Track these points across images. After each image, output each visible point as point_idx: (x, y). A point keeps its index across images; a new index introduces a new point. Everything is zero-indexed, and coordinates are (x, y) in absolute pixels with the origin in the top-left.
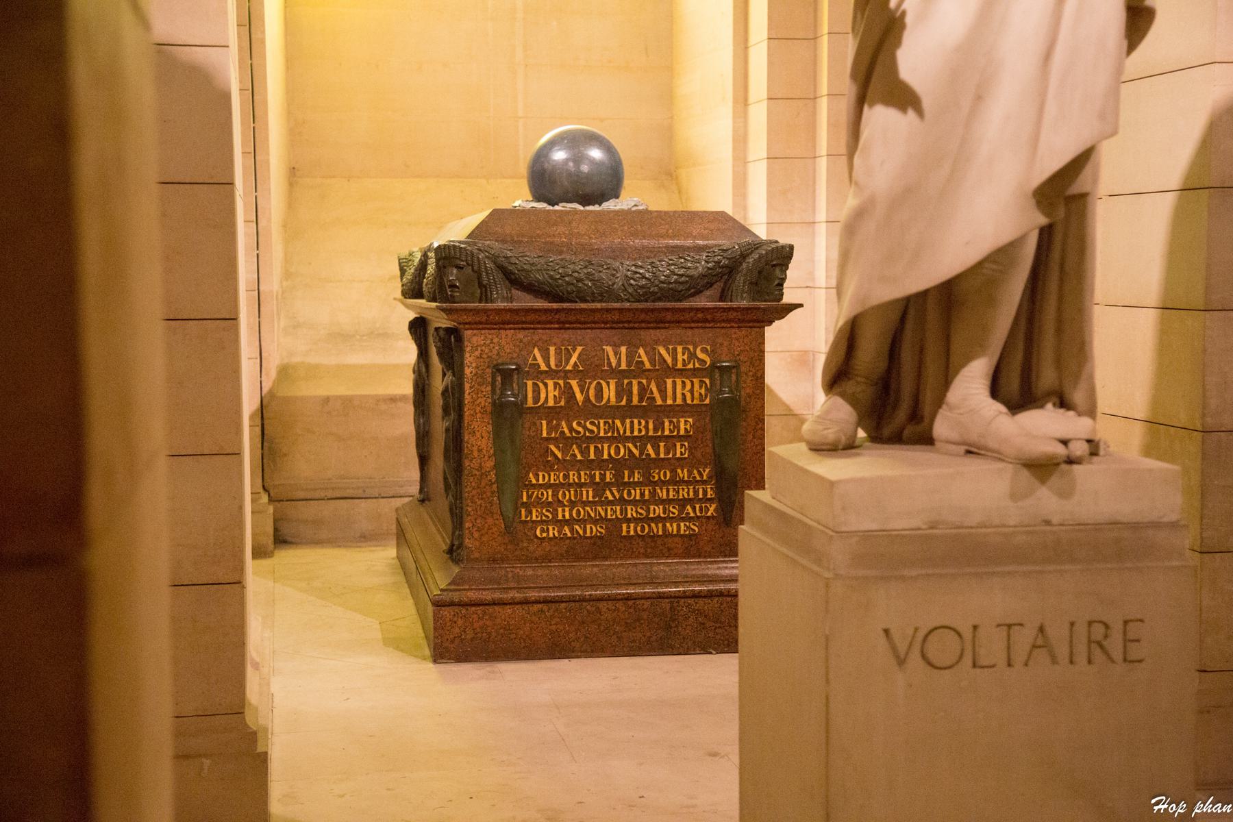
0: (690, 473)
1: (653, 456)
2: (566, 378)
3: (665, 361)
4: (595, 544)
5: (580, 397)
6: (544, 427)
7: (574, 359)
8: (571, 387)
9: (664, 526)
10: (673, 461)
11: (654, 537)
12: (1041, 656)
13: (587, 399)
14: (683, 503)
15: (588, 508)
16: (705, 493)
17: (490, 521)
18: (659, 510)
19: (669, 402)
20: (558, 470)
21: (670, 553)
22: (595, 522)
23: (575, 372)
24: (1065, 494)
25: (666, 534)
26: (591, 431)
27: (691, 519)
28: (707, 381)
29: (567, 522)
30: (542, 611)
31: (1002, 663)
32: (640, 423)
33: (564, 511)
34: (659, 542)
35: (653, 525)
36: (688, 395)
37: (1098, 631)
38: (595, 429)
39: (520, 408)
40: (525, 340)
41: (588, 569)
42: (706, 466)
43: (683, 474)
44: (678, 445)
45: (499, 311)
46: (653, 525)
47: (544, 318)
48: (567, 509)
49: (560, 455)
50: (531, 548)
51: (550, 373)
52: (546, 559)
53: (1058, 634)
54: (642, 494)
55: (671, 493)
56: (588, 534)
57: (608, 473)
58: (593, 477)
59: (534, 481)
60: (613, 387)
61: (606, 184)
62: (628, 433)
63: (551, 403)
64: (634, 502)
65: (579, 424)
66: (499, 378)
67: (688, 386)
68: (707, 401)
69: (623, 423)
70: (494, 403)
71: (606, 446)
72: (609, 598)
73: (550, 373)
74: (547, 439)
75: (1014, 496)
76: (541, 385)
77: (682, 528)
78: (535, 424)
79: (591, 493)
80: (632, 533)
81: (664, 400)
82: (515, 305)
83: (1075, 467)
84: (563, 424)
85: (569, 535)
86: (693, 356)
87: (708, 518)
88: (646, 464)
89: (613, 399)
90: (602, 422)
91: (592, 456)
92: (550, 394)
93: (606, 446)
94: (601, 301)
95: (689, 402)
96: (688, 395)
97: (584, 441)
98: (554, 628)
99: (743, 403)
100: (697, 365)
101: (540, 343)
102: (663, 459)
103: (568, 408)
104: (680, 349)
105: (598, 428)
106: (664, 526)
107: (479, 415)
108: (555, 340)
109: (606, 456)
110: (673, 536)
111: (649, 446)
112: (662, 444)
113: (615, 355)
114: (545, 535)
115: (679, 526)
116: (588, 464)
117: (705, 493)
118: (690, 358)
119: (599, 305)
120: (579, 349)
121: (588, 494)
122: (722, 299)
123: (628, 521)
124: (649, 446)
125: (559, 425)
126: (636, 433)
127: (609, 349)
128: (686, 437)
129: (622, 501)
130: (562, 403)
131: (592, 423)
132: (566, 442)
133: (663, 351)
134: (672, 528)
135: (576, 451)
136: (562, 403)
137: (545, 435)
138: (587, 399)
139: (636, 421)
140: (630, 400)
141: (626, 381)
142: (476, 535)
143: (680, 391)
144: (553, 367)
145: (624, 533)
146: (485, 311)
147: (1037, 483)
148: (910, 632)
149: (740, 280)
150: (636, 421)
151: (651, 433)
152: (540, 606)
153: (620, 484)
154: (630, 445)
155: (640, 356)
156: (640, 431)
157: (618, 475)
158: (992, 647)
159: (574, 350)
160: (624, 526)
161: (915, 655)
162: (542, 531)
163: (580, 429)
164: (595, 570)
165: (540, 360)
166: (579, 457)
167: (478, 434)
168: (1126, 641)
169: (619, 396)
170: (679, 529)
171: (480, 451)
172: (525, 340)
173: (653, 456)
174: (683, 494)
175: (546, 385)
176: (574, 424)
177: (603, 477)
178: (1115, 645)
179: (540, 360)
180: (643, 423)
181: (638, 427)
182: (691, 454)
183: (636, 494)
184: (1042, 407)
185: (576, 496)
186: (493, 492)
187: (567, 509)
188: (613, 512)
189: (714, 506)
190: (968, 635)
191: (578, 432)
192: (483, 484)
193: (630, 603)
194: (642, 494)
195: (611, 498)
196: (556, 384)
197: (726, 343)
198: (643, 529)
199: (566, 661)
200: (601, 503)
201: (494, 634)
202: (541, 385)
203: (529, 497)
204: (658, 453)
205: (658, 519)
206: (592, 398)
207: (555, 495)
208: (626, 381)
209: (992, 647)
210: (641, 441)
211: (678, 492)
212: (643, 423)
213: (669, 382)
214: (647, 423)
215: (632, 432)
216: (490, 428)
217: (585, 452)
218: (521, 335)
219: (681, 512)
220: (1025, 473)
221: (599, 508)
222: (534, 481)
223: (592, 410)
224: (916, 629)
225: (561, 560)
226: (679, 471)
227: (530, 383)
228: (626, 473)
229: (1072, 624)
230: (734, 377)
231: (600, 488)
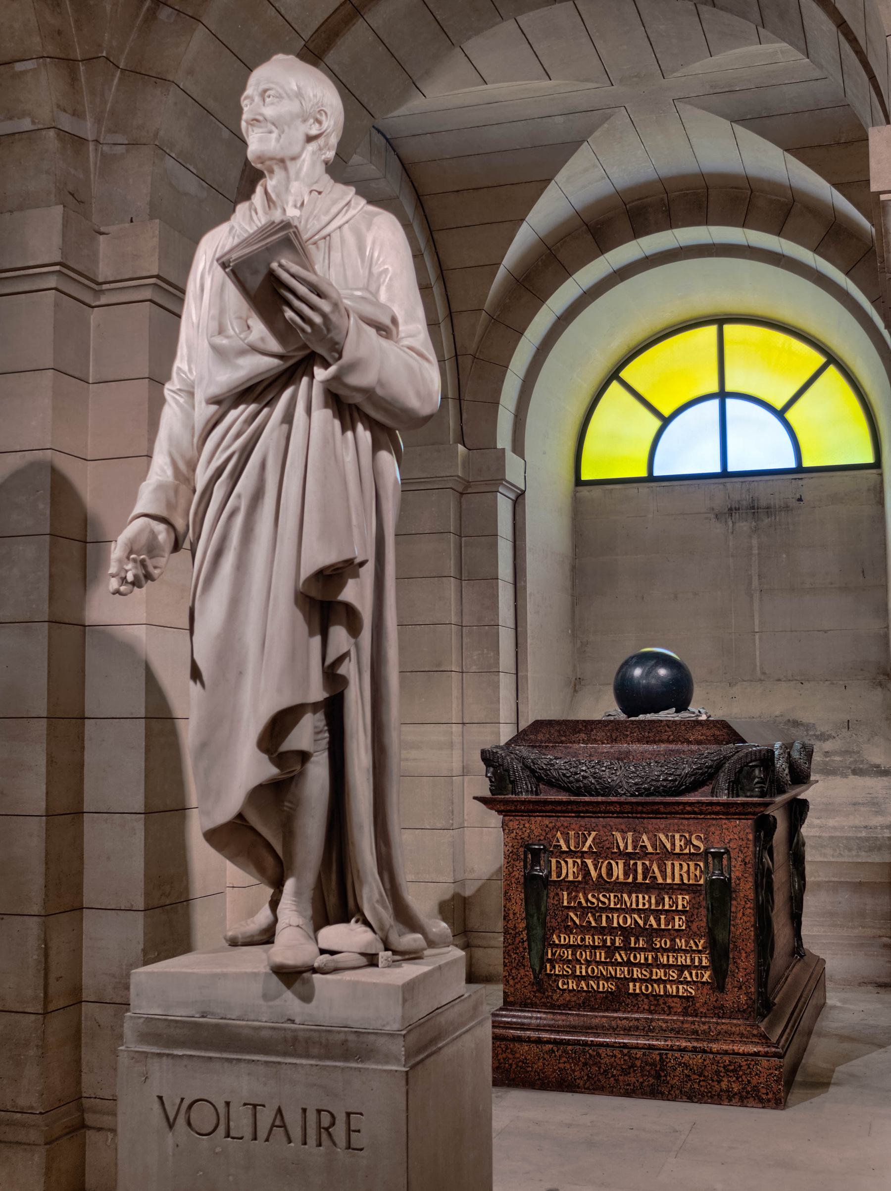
0: (687, 943)
1: (655, 926)
2: (582, 857)
3: (665, 847)
4: (606, 997)
5: (594, 874)
6: (565, 897)
7: (589, 842)
8: (587, 866)
9: (665, 987)
10: (672, 932)
11: (656, 996)
12: (279, 1132)
13: (600, 876)
14: (682, 968)
15: (601, 967)
16: (700, 960)
17: (522, 972)
18: (661, 973)
19: (669, 881)
20: (576, 933)
21: (670, 1011)
22: (607, 979)
23: (590, 852)
24: (307, 998)
25: (667, 995)
26: (604, 903)
27: (688, 983)
28: (702, 864)
29: (582, 978)
30: (553, 1051)
31: (248, 1135)
32: (644, 898)
33: (581, 968)
34: (661, 1001)
35: (655, 986)
36: (685, 876)
37: (326, 1120)
38: (606, 901)
39: (546, 882)
40: (550, 825)
41: (600, 1017)
42: (701, 938)
43: (681, 943)
44: (677, 918)
45: (523, 802)
46: (655, 986)
47: (559, 808)
48: (583, 967)
49: (577, 922)
50: (555, 997)
51: (570, 853)
52: (567, 1006)
53: (293, 1118)
54: (646, 959)
55: (671, 959)
56: (601, 990)
57: (617, 939)
58: (605, 941)
59: (557, 942)
60: (621, 865)
61: (678, 692)
62: (634, 906)
63: (571, 878)
64: (639, 965)
65: (593, 896)
66: (530, 856)
67: (685, 868)
68: (702, 882)
69: (630, 897)
70: (524, 876)
71: (615, 916)
72: (607, 1045)
73: (570, 853)
74: (567, 908)
75: (266, 997)
76: (562, 862)
77: (681, 990)
78: (557, 894)
79: (603, 954)
80: (638, 991)
81: (665, 879)
82: (542, 797)
83: (316, 977)
84: (581, 895)
85: (585, 989)
86: (689, 842)
87: (703, 983)
88: (651, 934)
89: (621, 877)
90: (612, 895)
91: (604, 924)
92: (570, 870)
93: (615, 916)
94: (603, 795)
95: (686, 881)
96: (685, 876)
97: (597, 911)
98: (562, 1066)
99: (733, 885)
100: (692, 851)
101: (562, 829)
102: (663, 930)
103: (584, 883)
104: (677, 836)
105: (609, 899)
106: (665, 987)
107: (514, 885)
108: (573, 826)
109: (615, 925)
110: (673, 996)
111: (652, 918)
112: (663, 917)
113: (624, 841)
114: (565, 987)
115: (678, 988)
116: (601, 931)
117: (700, 960)
118: (686, 844)
119: (600, 799)
120: (593, 834)
121: (601, 955)
122: (713, 794)
123: (634, 981)
124: (652, 918)
125: (576, 896)
126: (641, 906)
127: (618, 835)
128: (684, 912)
129: (629, 964)
130: (580, 879)
131: (604, 896)
132: (583, 911)
133: (663, 837)
134: (672, 989)
135: (591, 919)
136: (580, 879)
137: (565, 904)
138: (600, 876)
139: (640, 896)
140: (635, 878)
141: (632, 862)
142: (511, 982)
143: (678, 872)
144: (572, 848)
145: (631, 991)
146: (513, 802)
147: (284, 988)
148: (178, 1101)
149: (722, 777)
150: (640, 896)
151: (653, 907)
152: (551, 1046)
153: (627, 948)
154: (636, 916)
155: (643, 842)
156: (644, 904)
157: (626, 941)
158: (241, 1122)
159: (589, 835)
160: (631, 985)
161: (181, 1121)
162: (564, 984)
163: (594, 900)
164: (604, 1020)
165: (562, 843)
166: (593, 924)
167: (513, 901)
168: (349, 1131)
169: (626, 875)
170: (678, 991)
171: (514, 914)
172: (550, 825)
173: (655, 926)
174: (682, 960)
175: (566, 862)
176: (590, 896)
177: (613, 942)
178: (339, 1131)
179: (562, 843)
180: (647, 897)
181: (643, 901)
182: (688, 927)
183: (641, 958)
184: (348, 921)
185: (591, 956)
186: (525, 949)
187: (583, 967)
188: (621, 972)
189: (708, 973)
190: (222, 1110)
191: (593, 903)
192: (517, 941)
193: (626, 1051)
194: (646, 959)
195: (620, 960)
196: (574, 862)
197: (718, 832)
198: (647, 987)
199: (570, 1094)
200: (612, 964)
201: (514, 1066)
202: (562, 862)
203: (553, 954)
204: (659, 924)
205: (659, 981)
206: (604, 875)
207: (574, 954)
208: (632, 862)
209: (241, 1122)
210: (645, 913)
211: (677, 959)
212: (647, 897)
213: (669, 863)
214: (650, 898)
215: (637, 905)
216: (523, 895)
217: (598, 920)
218: (546, 821)
219: (680, 976)
220: (275, 978)
221: (610, 968)
222: (557, 942)
223: (603, 885)
224: (182, 1099)
225: (579, 1010)
226: (678, 940)
227: (554, 861)
228: (633, 939)
229: (304, 1110)
230: (725, 862)
231: (611, 951)
